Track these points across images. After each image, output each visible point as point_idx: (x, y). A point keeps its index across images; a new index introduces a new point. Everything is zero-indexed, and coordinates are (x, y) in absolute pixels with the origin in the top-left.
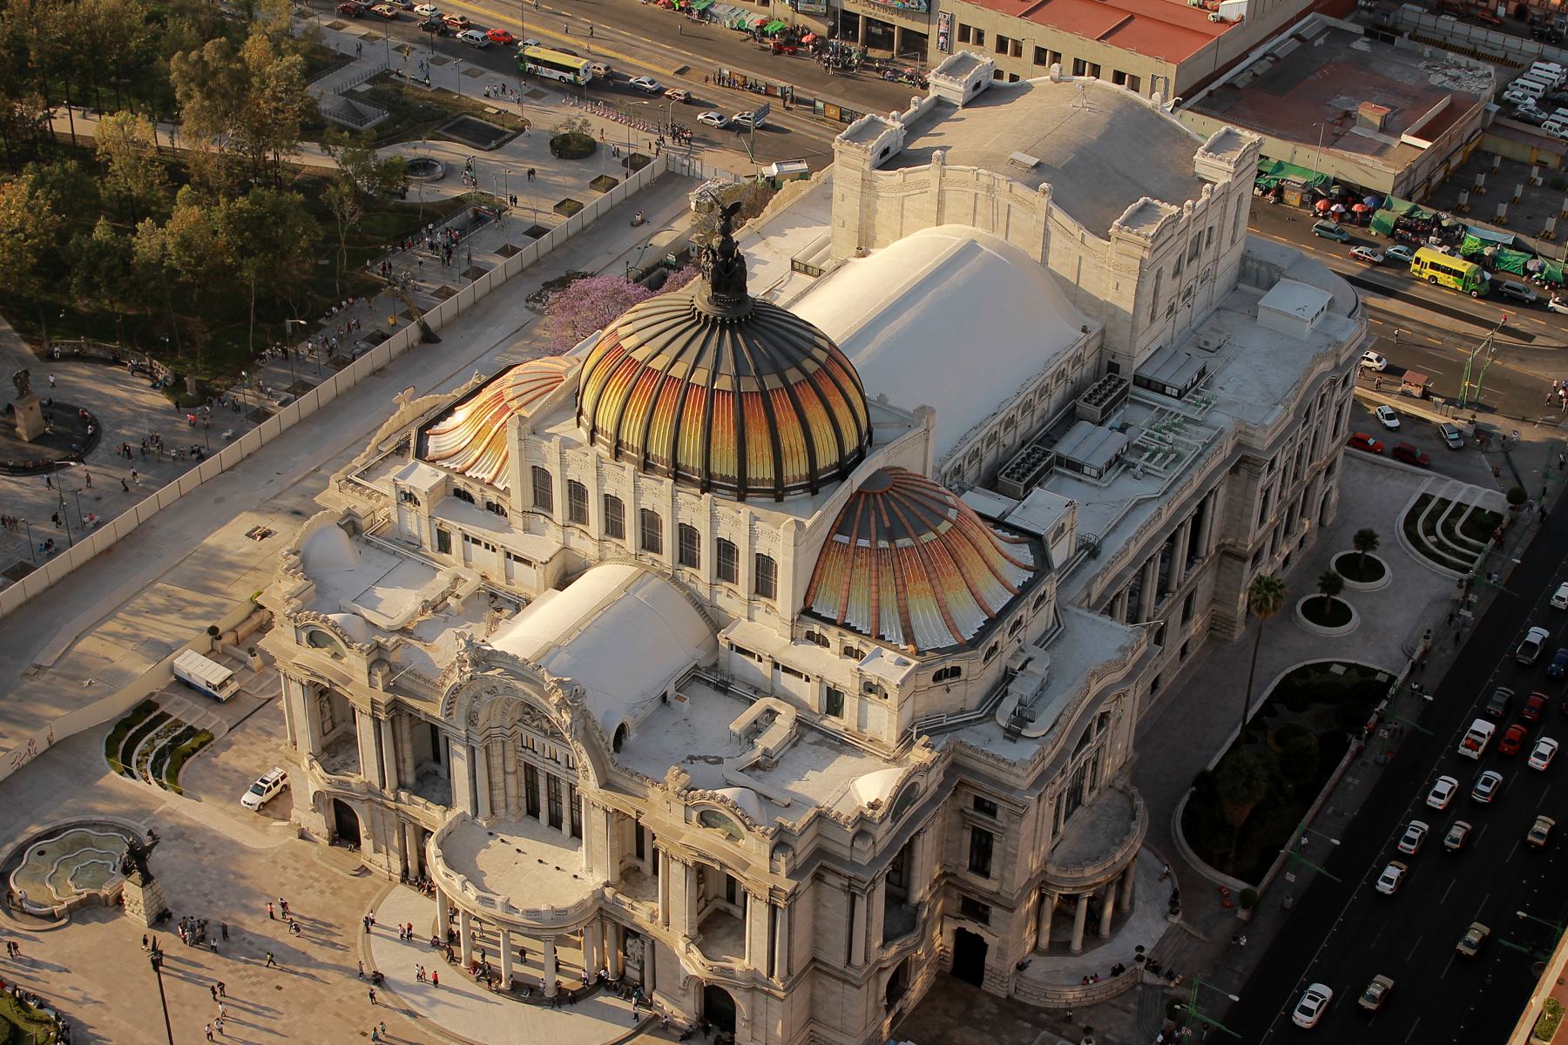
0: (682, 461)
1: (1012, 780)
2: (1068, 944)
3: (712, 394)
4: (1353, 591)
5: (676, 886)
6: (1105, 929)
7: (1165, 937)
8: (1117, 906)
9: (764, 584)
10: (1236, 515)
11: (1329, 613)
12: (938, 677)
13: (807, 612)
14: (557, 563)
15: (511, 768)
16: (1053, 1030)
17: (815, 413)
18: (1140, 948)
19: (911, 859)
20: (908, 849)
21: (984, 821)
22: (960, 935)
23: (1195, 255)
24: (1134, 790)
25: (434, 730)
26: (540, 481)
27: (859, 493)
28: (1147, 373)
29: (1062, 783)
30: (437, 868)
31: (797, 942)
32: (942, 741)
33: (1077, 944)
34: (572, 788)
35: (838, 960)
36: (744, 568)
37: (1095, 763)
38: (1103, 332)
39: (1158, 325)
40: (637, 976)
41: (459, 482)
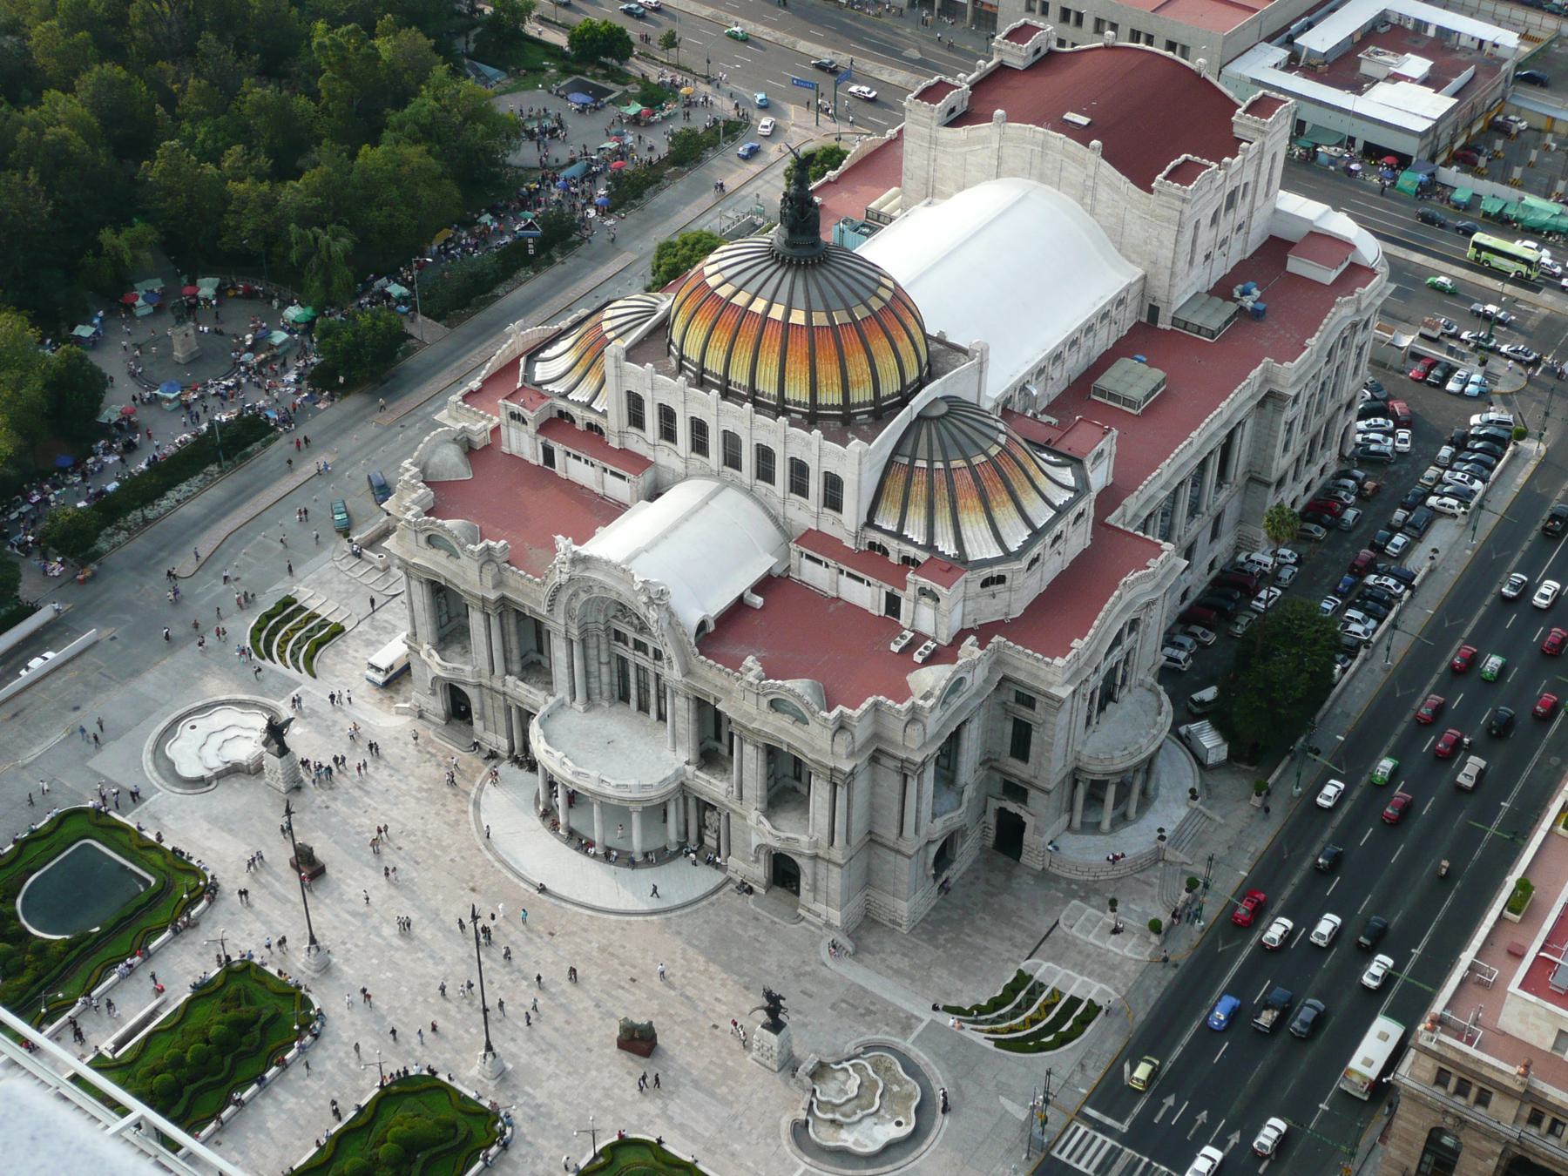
0: (760, 387)
1: (1050, 677)
2: (1099, 824)
3: (786, 326)
5: (750, 762)
7: (1186, 820)
9: (833, 500)
12: (985, 584)
13: (870, 523)
15: (604, 659)
16: (1082, 899)
18: (1161, 830)
19: (958, 745)
20: (955, 737)
22: (1002, 812)
24: (1161, 688)
26: (635, 406)
28: (1183, 316)
29: (1096, 681)
30: (538, 747)
31: (854, 817)
33: (1106, 825)
34: (658, 677)
35: (889, 833)
36: (815, 485)
37: (1126, 662)
38: (1145, 277)
39: (1195, 272)
40: (714, 844)
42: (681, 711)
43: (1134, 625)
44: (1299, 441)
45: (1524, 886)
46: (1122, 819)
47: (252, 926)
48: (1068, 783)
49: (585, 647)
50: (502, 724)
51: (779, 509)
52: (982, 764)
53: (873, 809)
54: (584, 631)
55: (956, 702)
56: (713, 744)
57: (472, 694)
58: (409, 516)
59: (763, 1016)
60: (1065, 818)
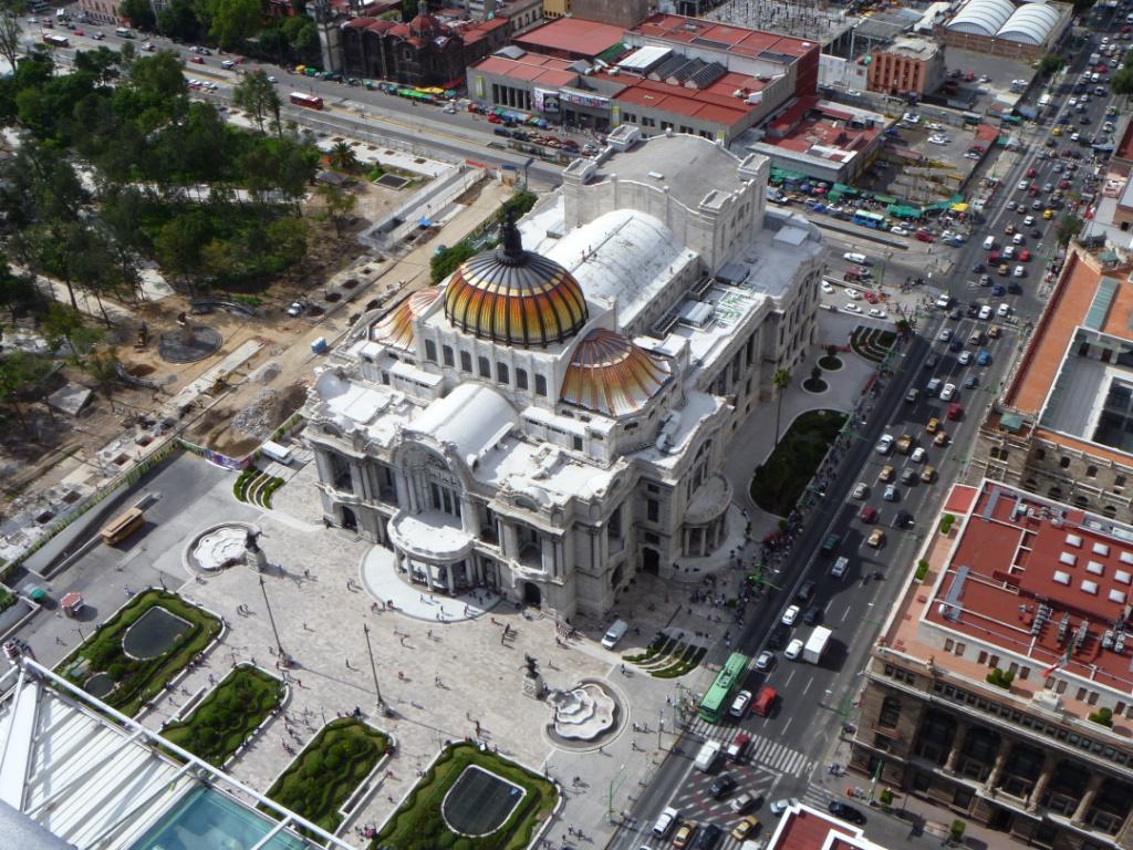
0: (497, 331)
4: (827, 376)
5: (506, 534)
6: (716, 545)
8: (721, 533)
10: (769, 341)
11: (816, 385)
12: (627, 427)
13: (562, 401)
14: (441, 386)
15: (425, 485)
17: (559, 304)
20: (617, 513)
21: (653, 495)
23: (741, 215)
25: (388, 470)
27: (584, 341)
28: (721, 275)
30: (393, 537)
32: (631, 459)
33: (703, 552)
35: (586, 566)
36: (531, 382)
41: (391, 350)
42: (466, 510)
43: (708, 443)
44: (788, 337)
45: (924, 564)
46: (711, 547)
47: (245, 646)
48: (680, 531)
49: (413, 478)
50: (373, 526)
51: (513, 398)
52: (634, 525)
53: (576, 554)
54: (413, 471)
55: (616, 493)
56: (487, 527)
57: (356, 511)
58: (313, 417)
59: (526, 671)
60: (680, 550)
